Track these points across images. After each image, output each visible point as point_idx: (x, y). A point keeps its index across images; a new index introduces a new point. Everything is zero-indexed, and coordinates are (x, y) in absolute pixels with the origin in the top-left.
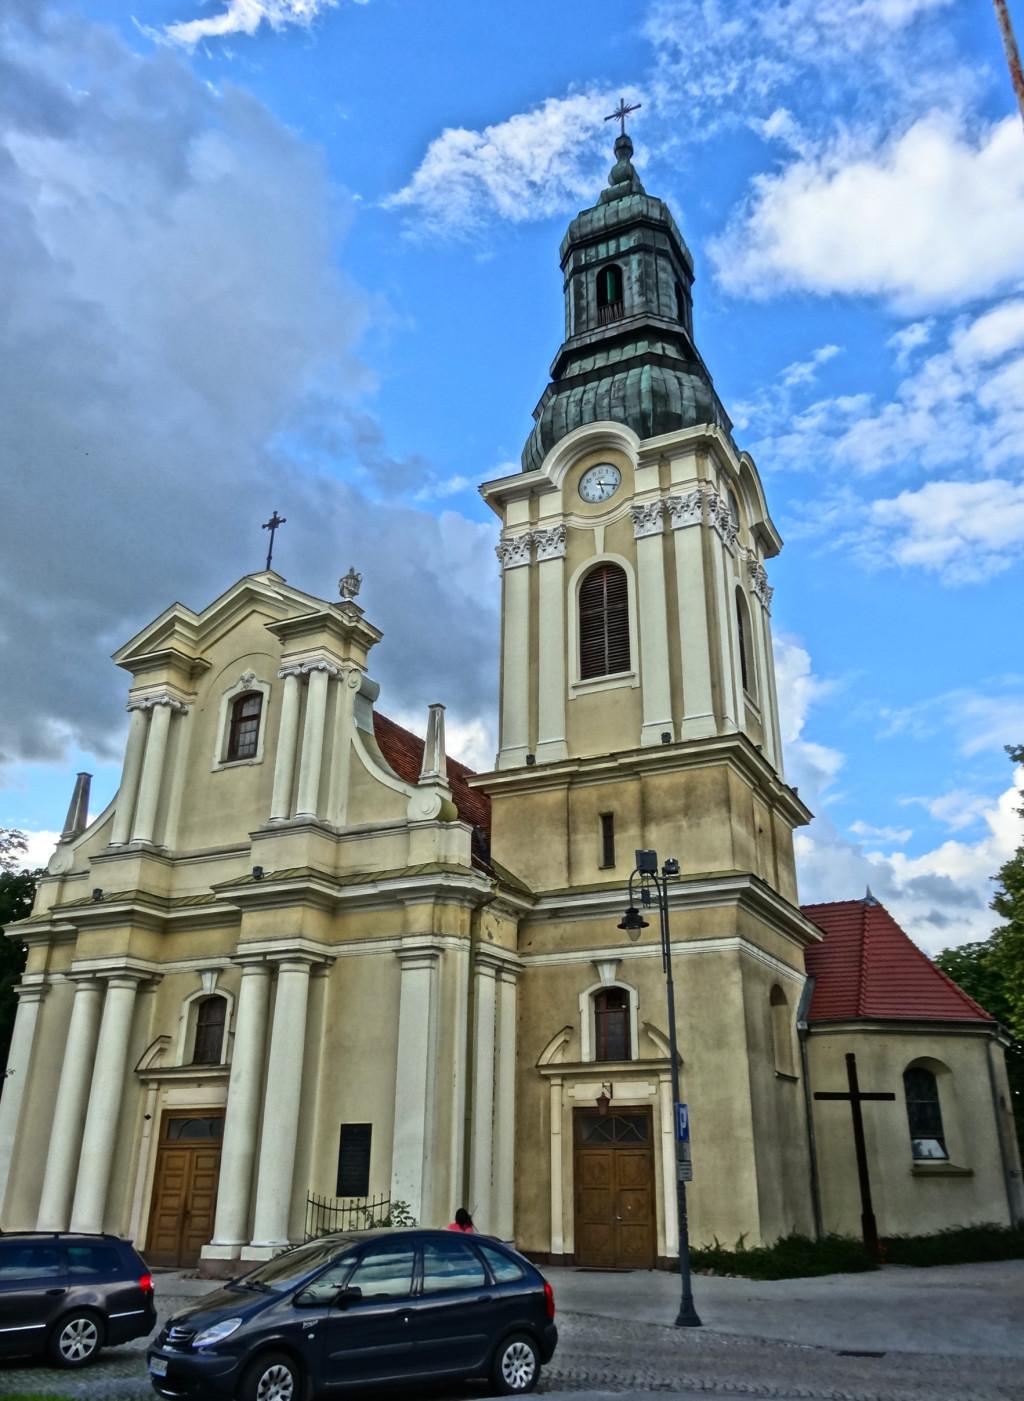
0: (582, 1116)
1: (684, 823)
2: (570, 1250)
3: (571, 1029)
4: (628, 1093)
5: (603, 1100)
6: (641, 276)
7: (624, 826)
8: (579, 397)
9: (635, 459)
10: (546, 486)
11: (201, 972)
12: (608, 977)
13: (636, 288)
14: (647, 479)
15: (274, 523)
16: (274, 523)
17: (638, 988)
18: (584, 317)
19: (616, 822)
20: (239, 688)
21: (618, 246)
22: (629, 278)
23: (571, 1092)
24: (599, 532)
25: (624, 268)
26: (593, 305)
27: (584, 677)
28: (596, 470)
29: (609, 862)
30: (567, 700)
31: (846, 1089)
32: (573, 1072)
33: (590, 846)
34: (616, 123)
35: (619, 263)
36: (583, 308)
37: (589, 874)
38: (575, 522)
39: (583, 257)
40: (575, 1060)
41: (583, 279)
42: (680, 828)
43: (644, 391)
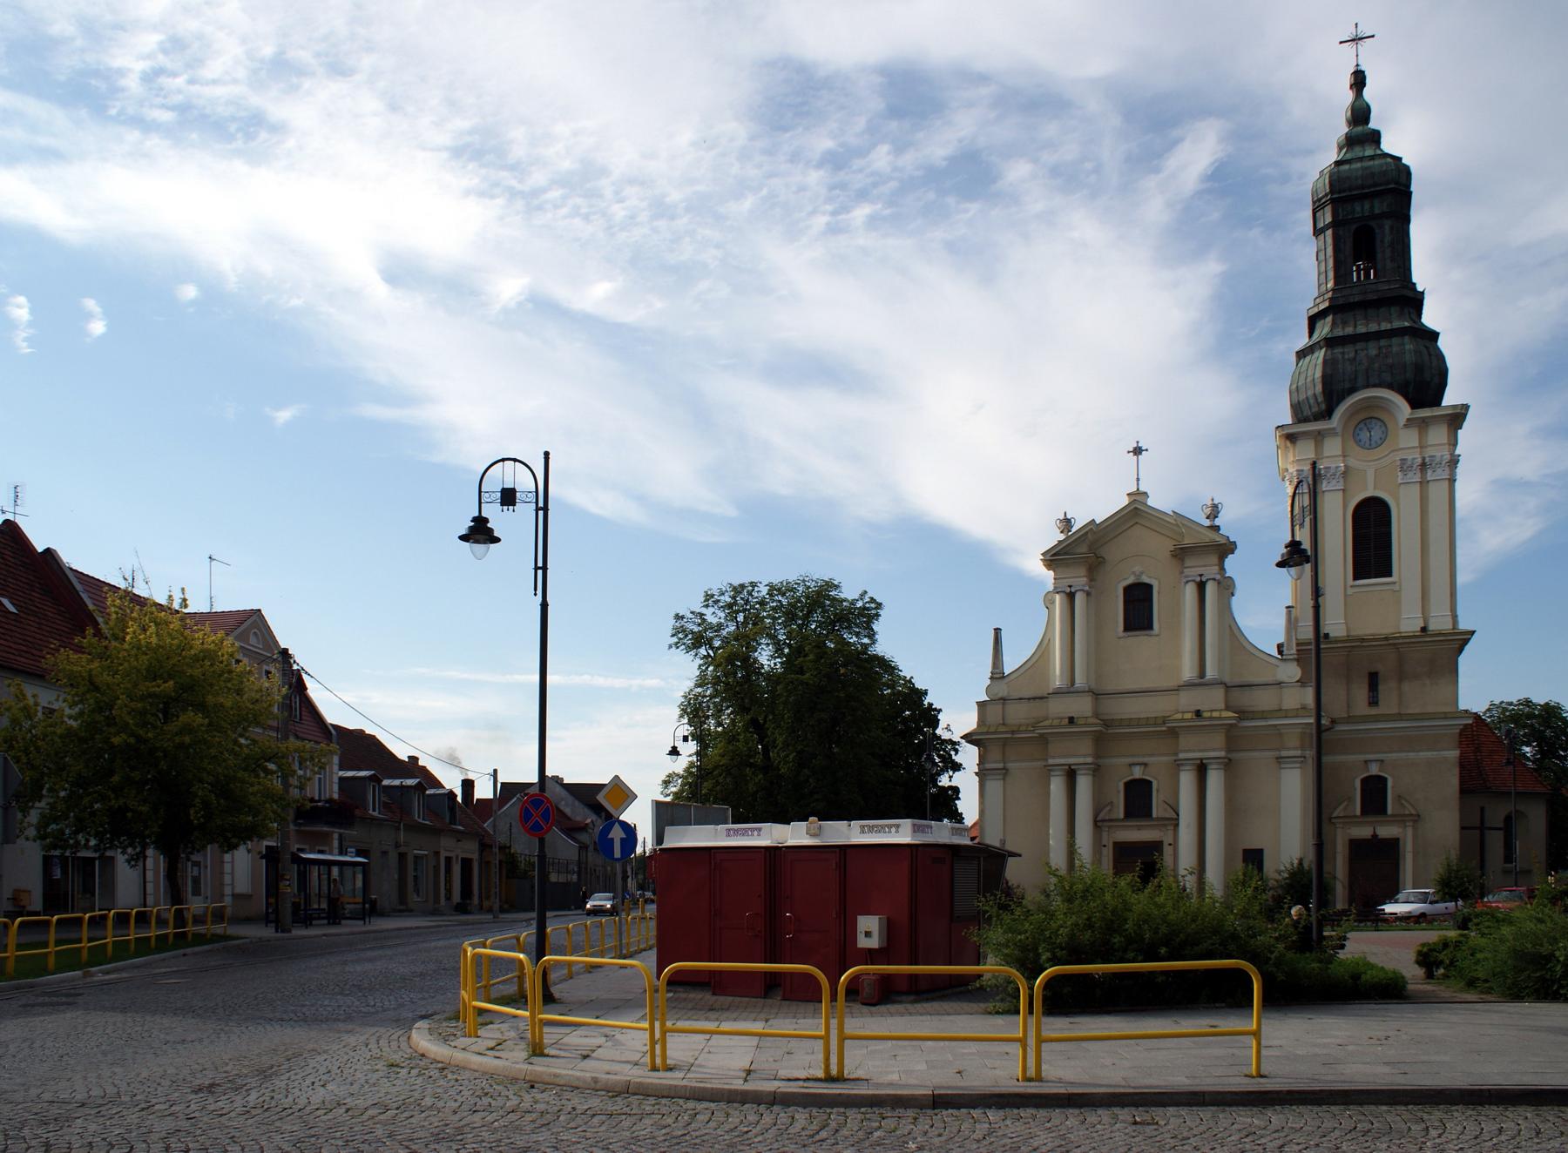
0: (1356, 846)
3: (1351, 799)
4: (1385, 832)
5: (1375, 836)
10: (1332, 432)
12: (1374, 770)
13: (1388, 253)
15: (1138, 451)
16: (1138, 451)
20: (1131, 580)
21: (1372, 207)
29: (1373, 702)
31: (1478, 824)
33: (1361, 693)
35: (1373, 224)
38: (1352, 462)
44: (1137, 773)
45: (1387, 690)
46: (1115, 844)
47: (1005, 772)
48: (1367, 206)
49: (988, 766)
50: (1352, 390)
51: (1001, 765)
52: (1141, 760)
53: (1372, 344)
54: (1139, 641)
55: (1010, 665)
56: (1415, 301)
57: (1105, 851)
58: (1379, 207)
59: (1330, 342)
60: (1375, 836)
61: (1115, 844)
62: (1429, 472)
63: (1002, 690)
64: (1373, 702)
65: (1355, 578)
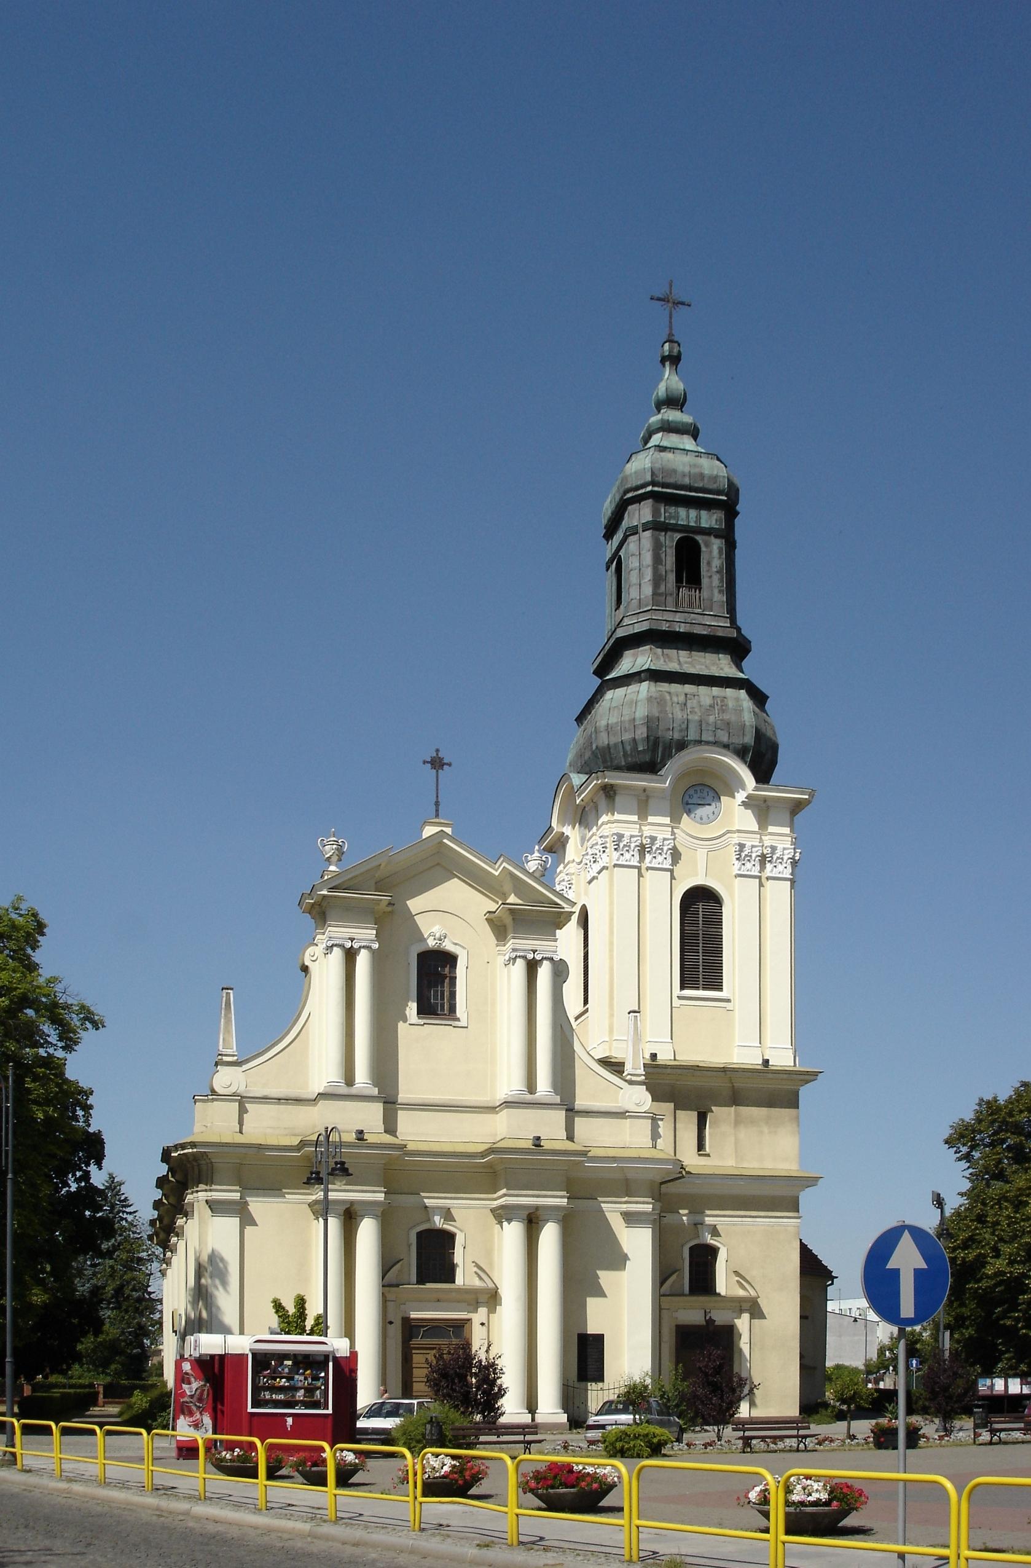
6: (721, 568)
8: (682, 698)
9: (741, 796)
13: (716, 581)
14: (747, 820)
18: (662, 589)
21: (698, 518)
22: (709, 563)
24: (701, 854)
25: (703, 549)
26: (672, 577)
28: (698, 788)
35: (699, 538)
36: (661, 575)
41: (662, 539)
43: (747, 724)
50: (682, 745)
53: (703, 690)
54: (435, 1032)
58: (709, 519)
59: (656, 676)
60: (710, 1322)
62: (769, 866)
65: (682, 988)
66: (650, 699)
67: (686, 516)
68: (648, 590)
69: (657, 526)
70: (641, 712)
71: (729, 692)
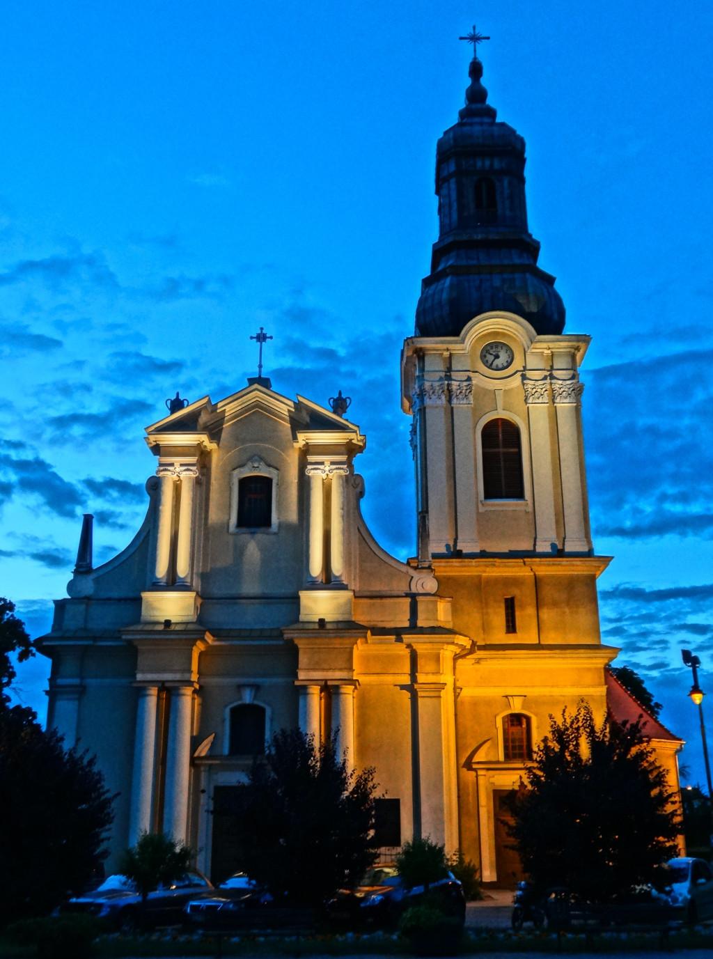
1: (567, 610)
2: (495, 879)
7: (523, 607)
11: (240, 687)
15: (261, 338)
16: (261, 338)
17: (536, 715)
19: (517, 603)
23: (492, 780)
27: (488, 495)
29: (511, 627)
30: (478, 513)
32: (492, 766)
33: (499, 619)
34: (468, 46)
37: (500, 637)
39: (464, 163)
40: (494, 760)
42: (564, 613)
44: (247, 697)
45: (526, 615)
46: (218, 789)
47: (80, 692)
48: (487, 163)
49: (60, 681)
51: (76, 681)
52: (252, 680)
55: (97, 562)
56: (532, 249)
57: (203, 799)
59: (454, 271)
61: (218, 789)
63: (88, 587)
64: (511, 627)
66: (451, 285)
67: (482, 164)
68: (455, 216)
69: (459, 173)
70: (445, 296)
71: (517, 276)
